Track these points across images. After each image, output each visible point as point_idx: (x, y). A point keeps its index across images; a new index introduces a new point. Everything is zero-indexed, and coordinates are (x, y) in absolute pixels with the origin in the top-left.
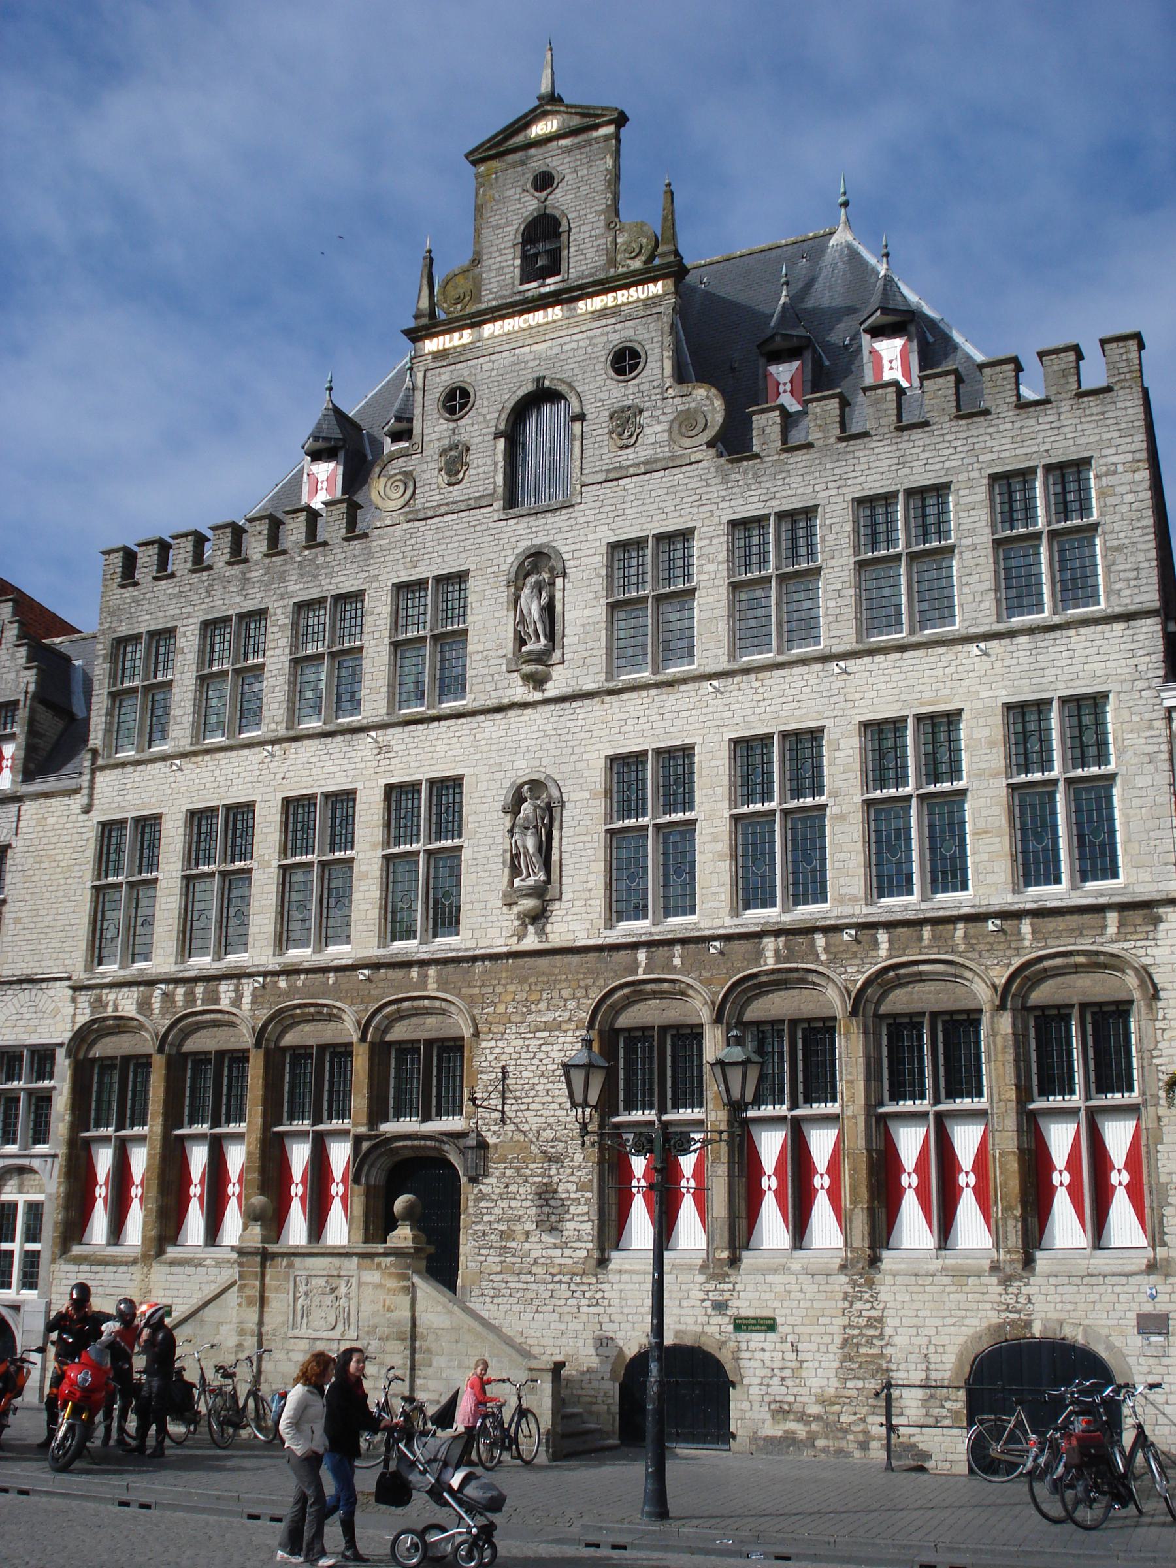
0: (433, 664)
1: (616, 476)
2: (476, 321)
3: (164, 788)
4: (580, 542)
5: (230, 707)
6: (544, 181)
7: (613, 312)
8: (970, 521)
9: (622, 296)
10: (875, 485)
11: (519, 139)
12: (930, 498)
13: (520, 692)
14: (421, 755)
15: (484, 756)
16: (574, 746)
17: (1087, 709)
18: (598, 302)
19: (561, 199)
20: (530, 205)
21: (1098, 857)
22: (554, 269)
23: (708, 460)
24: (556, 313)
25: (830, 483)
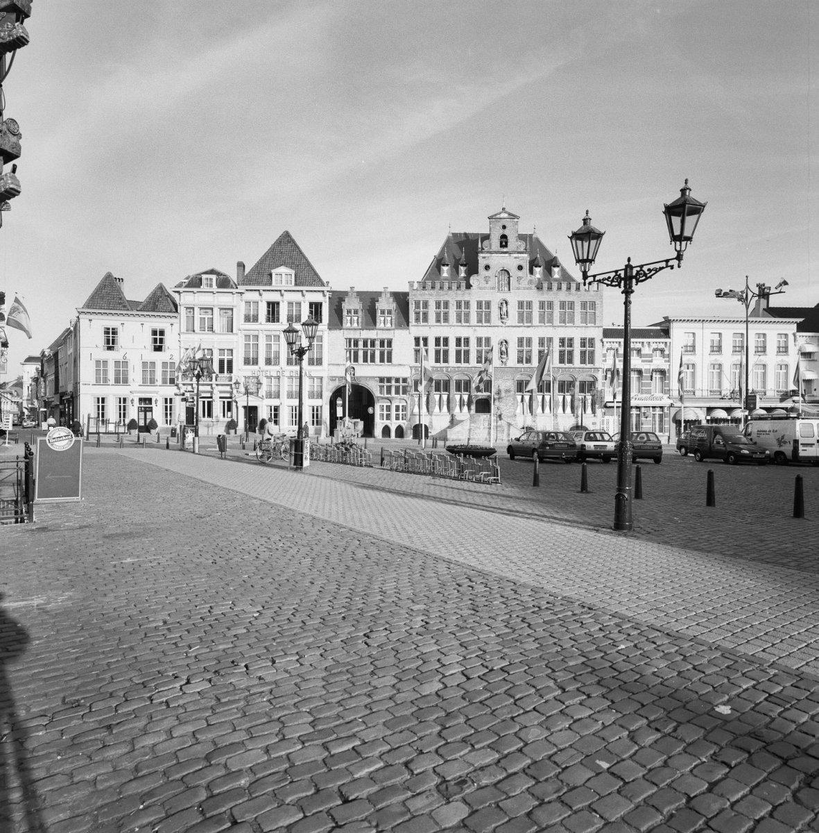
0: (484, 318)
1: (518, 289)
2: (491, 253)
3: (432, 331)
4: (513, 298)
5: (443, 318)
6: (504, 227)
7: (518, 258)
8: (578, 308)
9: (519, 255)
10: (562, 299)
11: (498, 216)
12: (572, 304)
13: (501, 324)
14: (483, 332)
15: (496, 334)
16: (512, 336)
17: (592, 341)
18: (515, 255)
19: (506, 232)
20: (501, 232)
21: (592, 362)
22: (506, 246)
23: (535, 290)
24: (507, 255)
25: (557, 297)
